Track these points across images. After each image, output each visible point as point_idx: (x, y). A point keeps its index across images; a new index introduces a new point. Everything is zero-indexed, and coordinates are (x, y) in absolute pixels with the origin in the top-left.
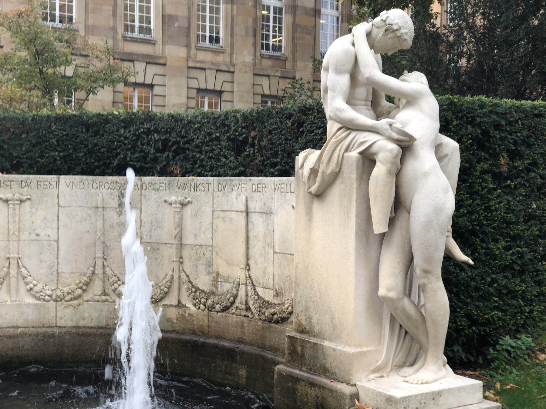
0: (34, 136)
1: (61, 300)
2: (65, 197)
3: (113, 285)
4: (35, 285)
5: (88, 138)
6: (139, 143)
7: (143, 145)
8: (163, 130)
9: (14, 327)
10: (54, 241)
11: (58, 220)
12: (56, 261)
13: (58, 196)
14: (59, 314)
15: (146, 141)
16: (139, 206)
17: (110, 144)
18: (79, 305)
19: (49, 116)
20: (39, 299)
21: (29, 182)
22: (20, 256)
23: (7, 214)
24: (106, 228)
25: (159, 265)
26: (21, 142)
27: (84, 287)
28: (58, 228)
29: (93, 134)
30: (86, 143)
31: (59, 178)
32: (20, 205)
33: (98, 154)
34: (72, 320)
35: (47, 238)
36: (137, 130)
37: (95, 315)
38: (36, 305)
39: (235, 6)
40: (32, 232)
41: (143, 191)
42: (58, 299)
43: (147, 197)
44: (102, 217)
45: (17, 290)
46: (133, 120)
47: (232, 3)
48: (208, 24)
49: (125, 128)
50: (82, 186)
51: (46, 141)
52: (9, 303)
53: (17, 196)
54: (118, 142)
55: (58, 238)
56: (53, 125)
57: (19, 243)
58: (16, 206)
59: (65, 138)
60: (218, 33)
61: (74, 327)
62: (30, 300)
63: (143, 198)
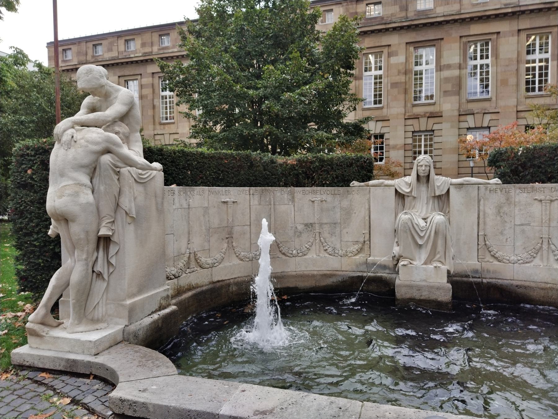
9: (545, 283)
22: (550, 237)
23: (541, 210)
26: (554, 162)
32: (550, 203)
45: (548, 259)
52: (541, 266)
53: (547, 198)
57: (549, 229)
58: (548, 204)
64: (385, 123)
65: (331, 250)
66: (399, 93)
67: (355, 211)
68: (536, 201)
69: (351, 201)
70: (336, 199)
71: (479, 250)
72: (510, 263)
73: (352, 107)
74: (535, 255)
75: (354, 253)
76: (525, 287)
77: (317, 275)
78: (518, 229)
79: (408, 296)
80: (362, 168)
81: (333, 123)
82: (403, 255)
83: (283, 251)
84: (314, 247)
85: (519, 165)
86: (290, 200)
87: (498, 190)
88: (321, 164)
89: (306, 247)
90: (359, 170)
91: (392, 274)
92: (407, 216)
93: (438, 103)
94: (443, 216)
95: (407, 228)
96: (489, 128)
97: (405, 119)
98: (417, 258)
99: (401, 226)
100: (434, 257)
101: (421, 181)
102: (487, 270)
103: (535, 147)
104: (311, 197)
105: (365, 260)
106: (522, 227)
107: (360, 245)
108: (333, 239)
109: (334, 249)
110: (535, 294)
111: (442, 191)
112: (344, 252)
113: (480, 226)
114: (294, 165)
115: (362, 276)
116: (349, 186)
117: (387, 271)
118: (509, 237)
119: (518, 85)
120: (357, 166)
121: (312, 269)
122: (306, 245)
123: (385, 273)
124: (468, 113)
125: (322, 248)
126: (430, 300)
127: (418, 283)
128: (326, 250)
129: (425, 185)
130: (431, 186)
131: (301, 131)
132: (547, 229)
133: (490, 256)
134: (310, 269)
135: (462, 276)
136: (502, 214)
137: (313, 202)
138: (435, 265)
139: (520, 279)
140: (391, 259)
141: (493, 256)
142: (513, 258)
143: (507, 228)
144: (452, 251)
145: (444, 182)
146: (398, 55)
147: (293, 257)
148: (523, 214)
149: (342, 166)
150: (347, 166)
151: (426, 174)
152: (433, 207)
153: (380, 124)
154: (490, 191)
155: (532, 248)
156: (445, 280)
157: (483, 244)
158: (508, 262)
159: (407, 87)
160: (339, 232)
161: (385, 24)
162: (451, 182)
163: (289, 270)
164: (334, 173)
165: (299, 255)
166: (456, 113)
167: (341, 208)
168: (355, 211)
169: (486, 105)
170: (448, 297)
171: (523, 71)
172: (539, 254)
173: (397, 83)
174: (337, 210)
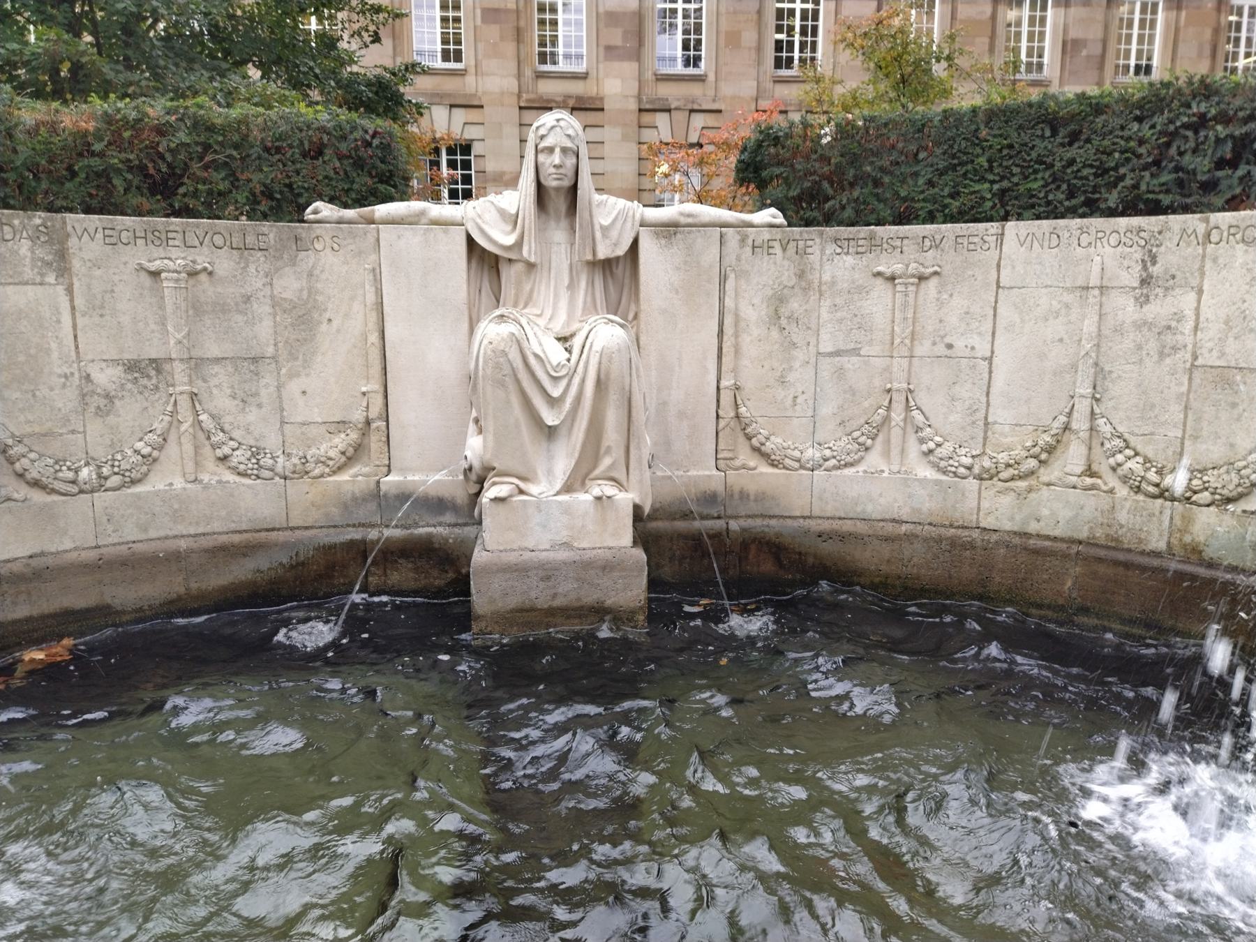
0: (944, 154)
1: (991, 479)
2: (1014, 267)
3: (1114, 455)
4: (939, 445)
5: (1055, 150)
6: (1173, 151)
7: (1181, 154)
8: (1241, 114)
9: (894, 521)
10: (984, 359)
11: (995, 315)
12: (984, 399)
13: (999, 266)
14: (985, 504)
15: (1192, 144)
16: (1195, 283)
17: (1104, 157)
18: (1030, 490)
19: (974, 111)
20: (944, 473)
21: (938, 237)
23: (890, 306)
24: (1106, 332)
25: (1238, 419)
27: (1044, 456)
28: (994, 334)
29: (1066, 140)
30: (1049, 160)
31: (1003, 227)
32: (918, 285)
33: (1075, 181)
34: (1012, 519)
35: (967, 353)
36: (1171, 121)
37: (1065, 514)
38: (937, 482)
39: (1184, 13)
40: (938, 340)
41: (1210, 247)
42: (985, 476)
43: (1221, 261)
44: (1097, 308)
45: (903, 451)
46: (1162, 100)
47: (1179, 8)
48: (1134, 47)
49: (1139, 120)
50: (1055, 242)
51: (967, 163)
53: (911, 270)
54: (1122, 152)
55: (993, 352)
56: (982, 127)
57: (910, 363)
58: (911, 288)
59: (1005, 152)
60: (1149, 59)
61: (1015, 533)
62: (929, 473)
63: (1208, 264)
64: (473, 115)
65: (242, 459)
66: (502, 38)
67: (327, 315)
68: (879, 281)
69: (310, 275)
70: (252, 269)
71: (721, 434)
72: (802, 467)
73: (367, 31)
74: (869, 442)
75: (331, 463)
76: (843, 537)
77: (190, 552)
78: (826, 365)
79: (513, 602)
80: (359, 164)
81: (311, 68)
82: (495, 465)
83: (33, 474)
84: (172, 449)
85: (823, 177)
86: (49, 264)
87: (777, 245)
88: (202, 139)
89: (137, 452)
90: (346, 173)
91: (466, 525)
92: (507, 329)
93: (593, 74)
94: (622, 326)
95: (507, 371)
97: (521, 108)
98: (541, 473)
99: (485, 362)
100: (595, 467)
101: (551, 207)
102: (741, 492)
103: (869, 120)
104: (144, 255)
105: (373, 486)
106: (837, 359)
107: (354, 436)
108: (252, 415)
109: (256, 452)
110: (869, 558)
111: (615, 245)
112: (295, 460)
113: (724, 359)
114: (85, 134)
115: (364, 542)
117: (449, 518)
118: (800, 390)
119: (759, 49)
120: (341, 158)
121: (170, 533)
122: (139, 445)
123: (440, 524)
124: (656, 107)
125: (207, 450)
126: (582, 608)
127: (544, 556)
128: (225, 458)
129: (564, 223)
130: (581, 225)
131: (198, 74)
132: (905, 362)
133: (748, 450)
134: (162, 533)
135: (672, 517)
136: (784, 322)
137: (155, 274)
138: (596, 491)
139: (829, 515)
140: (461, 477)
141: (756, 450)
142: (812, 453)
143: (797, 364)
144: (647, 442)
145: (622, 216)
147: (81, 492)
148: (840, 321)
149: (278, 150)
150: (305, 155)
151: (567, 183)
152: (589, 299)
153: (460, 115)
154: (754, 247)
155: (862, 421)
156: (627, 538)
157: (732, 414)
158: (796, 465)
159: (522, 23)
160: (272, 389)
162: (642, 215)
163: (68, 545)
164: (256, 177)
165: (109, 484)
166: (633, 105)
167: (275, 303)
168: (327, 315)
169: (695, 90)
170: (635, 592)
171: (771, 21)
172: (880, 438)
173: (496, 10)
174: (262, 309)
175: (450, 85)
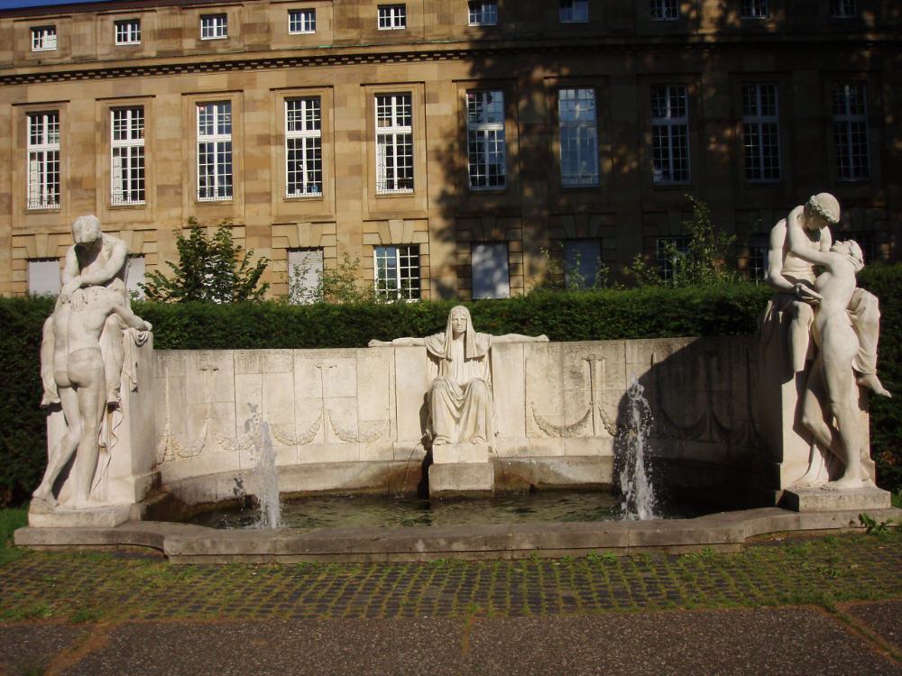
96: (600, 239)
116: (366, 345)
146: (438, 102)
161: (414, 44)
175: (403, 205)
